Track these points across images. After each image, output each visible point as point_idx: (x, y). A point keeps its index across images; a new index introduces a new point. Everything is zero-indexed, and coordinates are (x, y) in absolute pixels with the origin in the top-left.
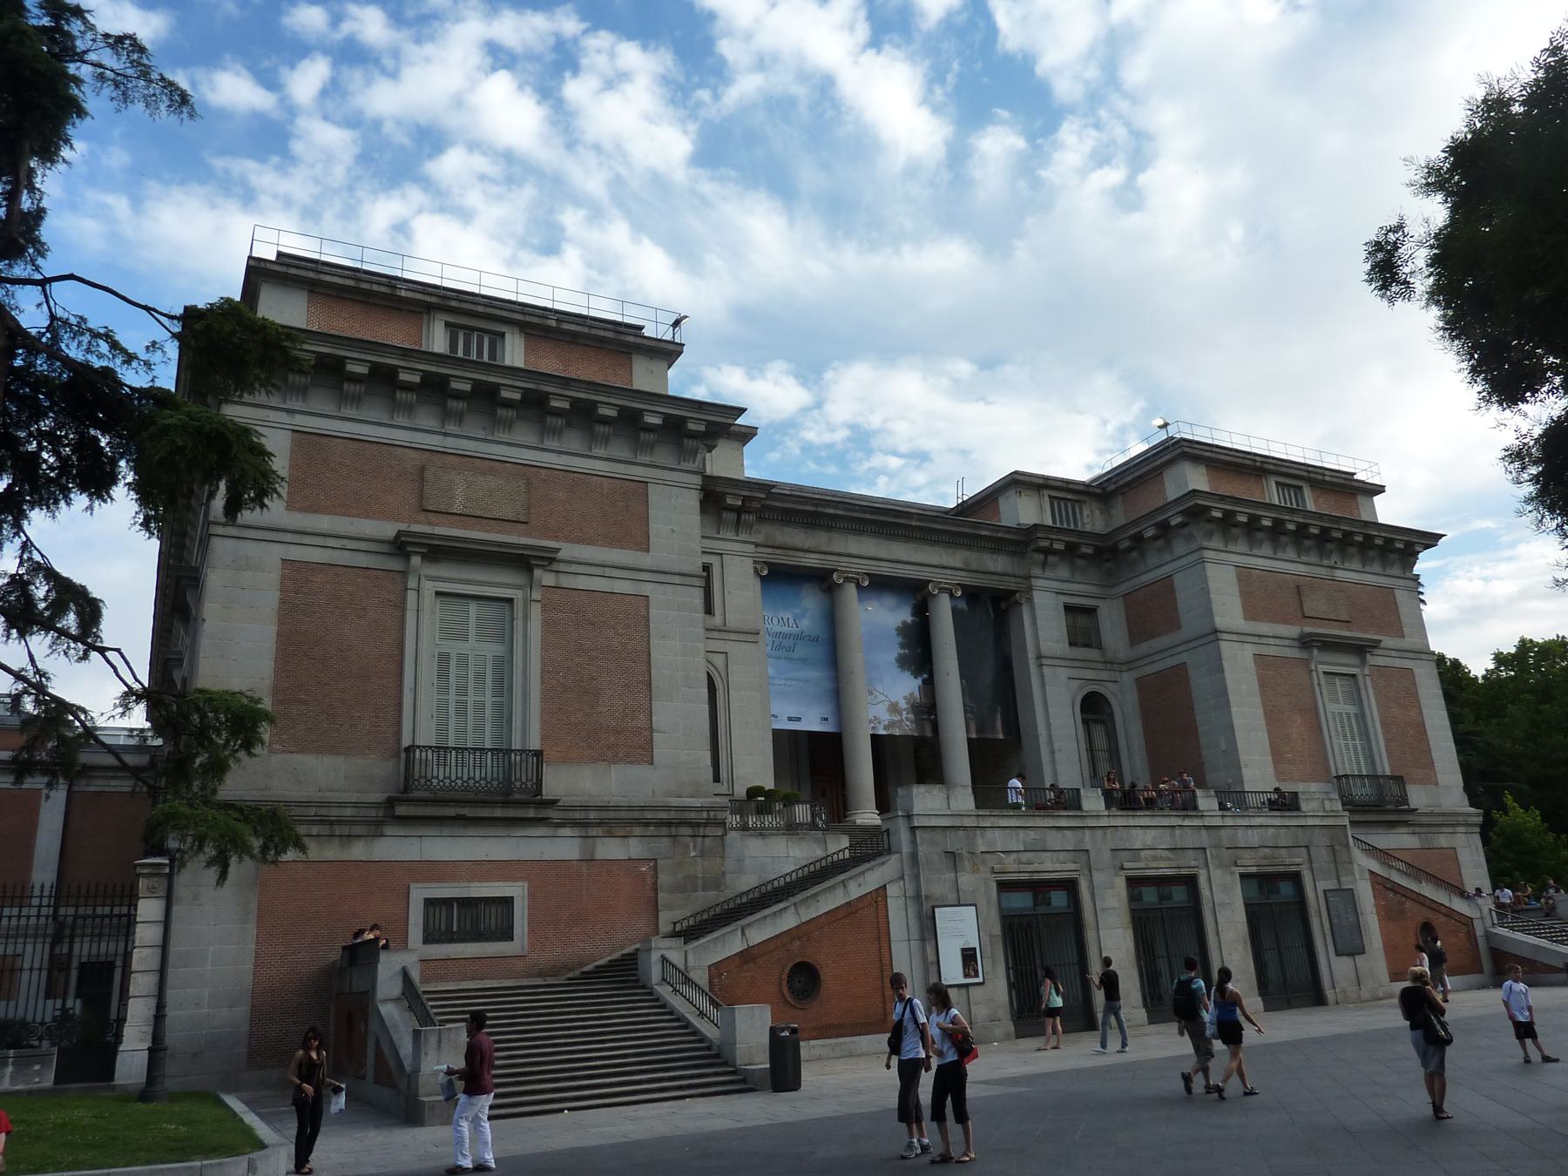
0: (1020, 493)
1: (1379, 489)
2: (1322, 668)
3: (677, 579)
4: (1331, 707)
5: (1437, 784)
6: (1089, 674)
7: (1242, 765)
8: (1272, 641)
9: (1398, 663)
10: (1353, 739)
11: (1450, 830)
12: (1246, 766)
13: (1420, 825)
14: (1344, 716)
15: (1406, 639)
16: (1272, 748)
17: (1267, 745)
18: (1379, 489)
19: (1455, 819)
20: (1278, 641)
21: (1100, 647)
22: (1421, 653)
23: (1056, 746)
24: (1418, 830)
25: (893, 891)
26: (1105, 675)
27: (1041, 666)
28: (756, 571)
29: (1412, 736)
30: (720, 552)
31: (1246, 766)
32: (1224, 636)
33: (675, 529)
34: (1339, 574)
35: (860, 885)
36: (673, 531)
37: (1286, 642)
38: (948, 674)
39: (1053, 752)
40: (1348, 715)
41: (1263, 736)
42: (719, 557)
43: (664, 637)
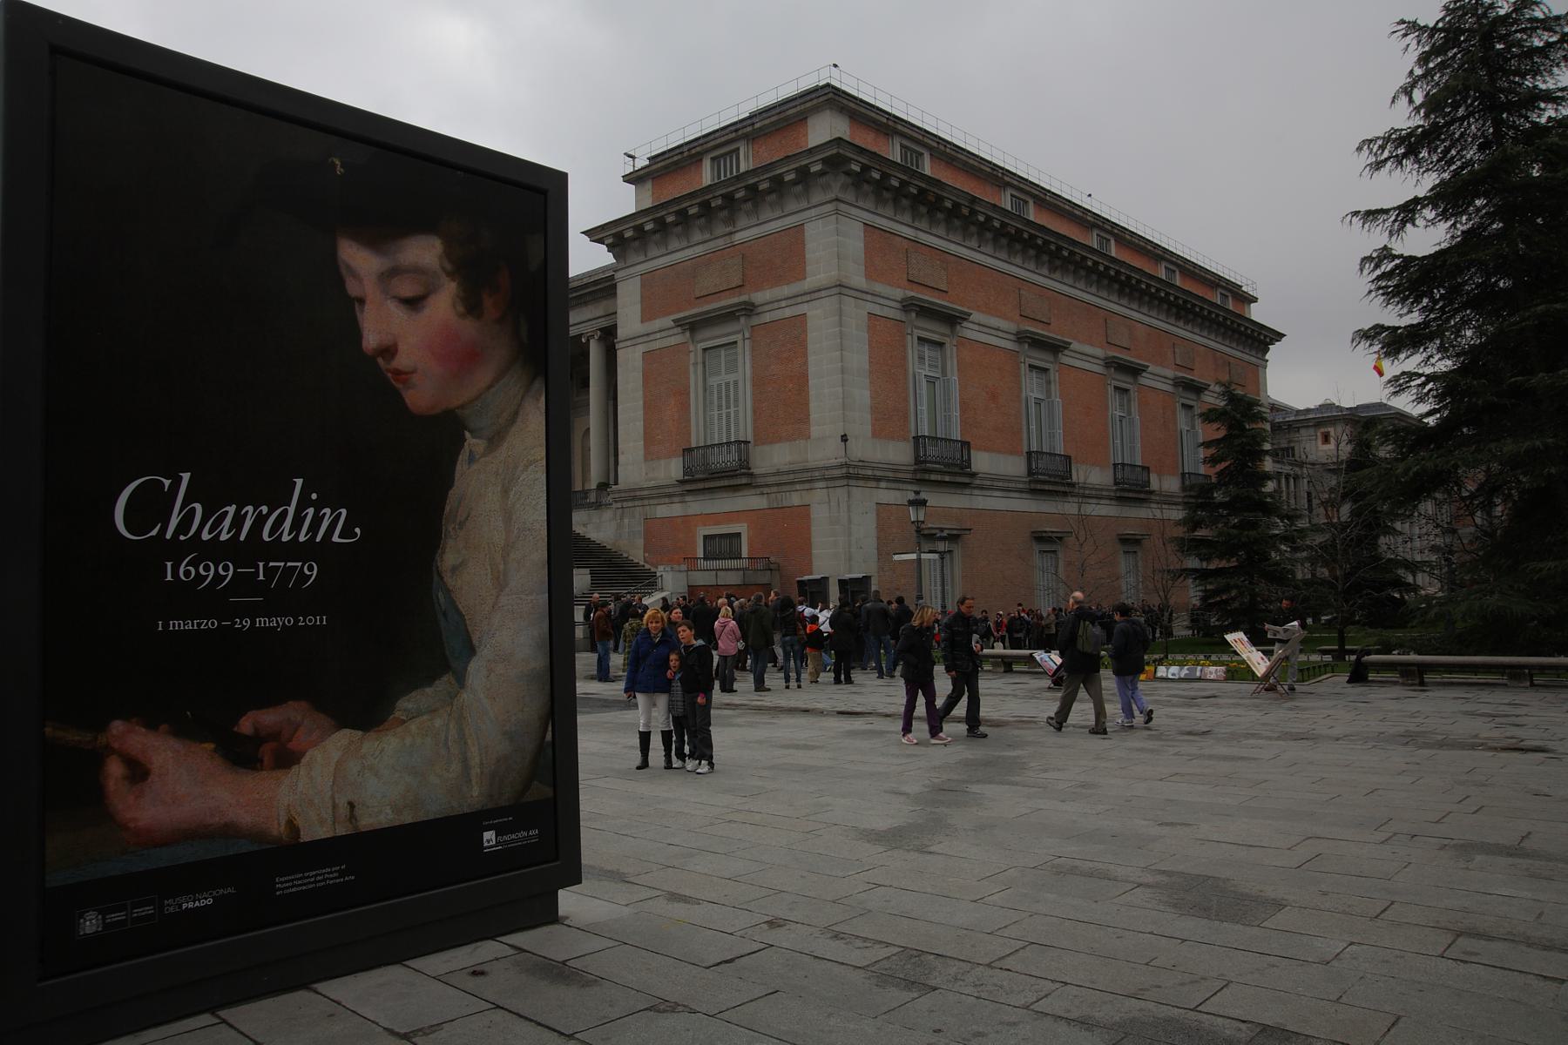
8: (658, 335)
9: (788, 313)
11: (807, 486)
12: (623, 453)
13: (767, 486)
14: (724, 387)
15: (808, 279)
16: (645, 433)
17: (642, 432)
19: (809, 474)
20: (663, 334)
22: (819, 290)
24: (766, 490)
34: (738, 237)
37: (671, 332)
40: (727, 384)
41: (640, 424)
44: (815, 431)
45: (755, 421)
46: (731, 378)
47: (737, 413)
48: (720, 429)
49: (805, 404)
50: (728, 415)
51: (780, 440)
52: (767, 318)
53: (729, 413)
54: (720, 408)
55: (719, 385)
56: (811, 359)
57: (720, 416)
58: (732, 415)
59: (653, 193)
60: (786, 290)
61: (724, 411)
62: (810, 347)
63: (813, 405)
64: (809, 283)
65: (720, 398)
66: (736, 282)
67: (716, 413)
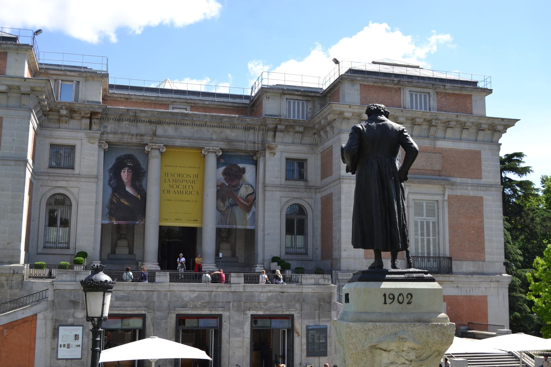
0: (269, 98)
1: (490, 91)
2: (412, 197)
3: (13, 163)
4: (419, 219)
5: (484, 261)
6: (295, 195)
7: (342, 250)
10: (428, 235)
14: (425, 224)
15: (483, 179)
18: (490, 91)
21: (306, 181)
23: (267, 232)
25: (40, 316)
26: (305, 195)
27: (264, 191)
28: (100, 146)
29: (472, 234)
30: (80, 138)
31: (345, 250)
32: (345, 181)
33: (14, 138)
34: (441, 144)
35: (23, 313)
36: (14, 140)
38: (208, 195)
39: (264, 235)
42: (80, 141)
43: (3, 190)
44: (488, 258)
45: (450, 247)
46: (432, 219)
47: (434, 240)
48: (423, 246)
49: (483, 243)
50: (428, 241)
51: (466, 260)
52: (459, 192)
53: (430, 239)
54: (422, 235)
55: (422, 223)
56: (486, 221)
57: (423, 240)
58: (431, 240)
59: (361, 94)
60: (470, 181)
61: (425, 238)
62: (485, 214)
63: (486, 244)
64: (483, 181)
65: (422, 229)
66: (438, 167)
67: (420, 237)
